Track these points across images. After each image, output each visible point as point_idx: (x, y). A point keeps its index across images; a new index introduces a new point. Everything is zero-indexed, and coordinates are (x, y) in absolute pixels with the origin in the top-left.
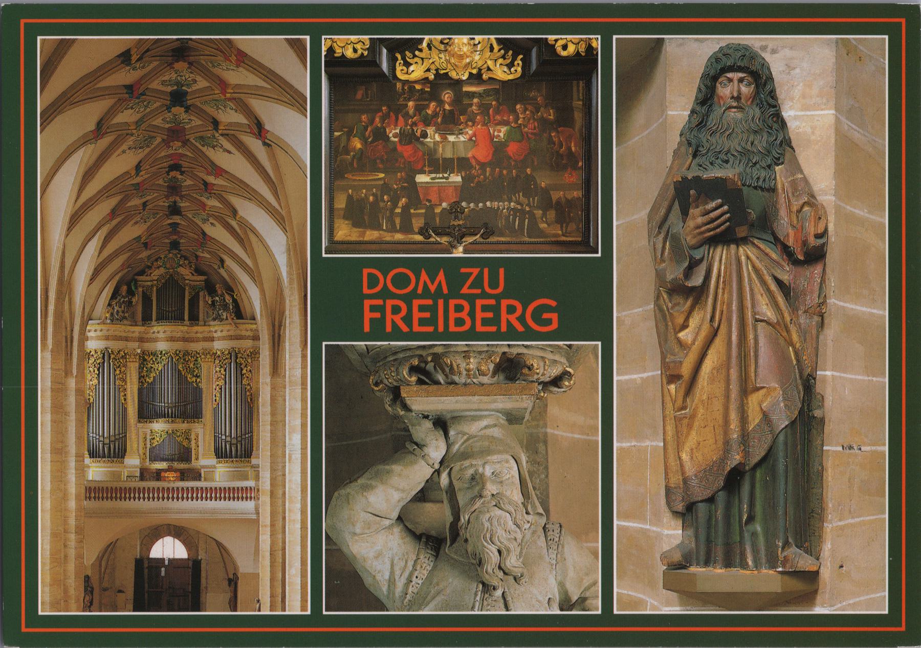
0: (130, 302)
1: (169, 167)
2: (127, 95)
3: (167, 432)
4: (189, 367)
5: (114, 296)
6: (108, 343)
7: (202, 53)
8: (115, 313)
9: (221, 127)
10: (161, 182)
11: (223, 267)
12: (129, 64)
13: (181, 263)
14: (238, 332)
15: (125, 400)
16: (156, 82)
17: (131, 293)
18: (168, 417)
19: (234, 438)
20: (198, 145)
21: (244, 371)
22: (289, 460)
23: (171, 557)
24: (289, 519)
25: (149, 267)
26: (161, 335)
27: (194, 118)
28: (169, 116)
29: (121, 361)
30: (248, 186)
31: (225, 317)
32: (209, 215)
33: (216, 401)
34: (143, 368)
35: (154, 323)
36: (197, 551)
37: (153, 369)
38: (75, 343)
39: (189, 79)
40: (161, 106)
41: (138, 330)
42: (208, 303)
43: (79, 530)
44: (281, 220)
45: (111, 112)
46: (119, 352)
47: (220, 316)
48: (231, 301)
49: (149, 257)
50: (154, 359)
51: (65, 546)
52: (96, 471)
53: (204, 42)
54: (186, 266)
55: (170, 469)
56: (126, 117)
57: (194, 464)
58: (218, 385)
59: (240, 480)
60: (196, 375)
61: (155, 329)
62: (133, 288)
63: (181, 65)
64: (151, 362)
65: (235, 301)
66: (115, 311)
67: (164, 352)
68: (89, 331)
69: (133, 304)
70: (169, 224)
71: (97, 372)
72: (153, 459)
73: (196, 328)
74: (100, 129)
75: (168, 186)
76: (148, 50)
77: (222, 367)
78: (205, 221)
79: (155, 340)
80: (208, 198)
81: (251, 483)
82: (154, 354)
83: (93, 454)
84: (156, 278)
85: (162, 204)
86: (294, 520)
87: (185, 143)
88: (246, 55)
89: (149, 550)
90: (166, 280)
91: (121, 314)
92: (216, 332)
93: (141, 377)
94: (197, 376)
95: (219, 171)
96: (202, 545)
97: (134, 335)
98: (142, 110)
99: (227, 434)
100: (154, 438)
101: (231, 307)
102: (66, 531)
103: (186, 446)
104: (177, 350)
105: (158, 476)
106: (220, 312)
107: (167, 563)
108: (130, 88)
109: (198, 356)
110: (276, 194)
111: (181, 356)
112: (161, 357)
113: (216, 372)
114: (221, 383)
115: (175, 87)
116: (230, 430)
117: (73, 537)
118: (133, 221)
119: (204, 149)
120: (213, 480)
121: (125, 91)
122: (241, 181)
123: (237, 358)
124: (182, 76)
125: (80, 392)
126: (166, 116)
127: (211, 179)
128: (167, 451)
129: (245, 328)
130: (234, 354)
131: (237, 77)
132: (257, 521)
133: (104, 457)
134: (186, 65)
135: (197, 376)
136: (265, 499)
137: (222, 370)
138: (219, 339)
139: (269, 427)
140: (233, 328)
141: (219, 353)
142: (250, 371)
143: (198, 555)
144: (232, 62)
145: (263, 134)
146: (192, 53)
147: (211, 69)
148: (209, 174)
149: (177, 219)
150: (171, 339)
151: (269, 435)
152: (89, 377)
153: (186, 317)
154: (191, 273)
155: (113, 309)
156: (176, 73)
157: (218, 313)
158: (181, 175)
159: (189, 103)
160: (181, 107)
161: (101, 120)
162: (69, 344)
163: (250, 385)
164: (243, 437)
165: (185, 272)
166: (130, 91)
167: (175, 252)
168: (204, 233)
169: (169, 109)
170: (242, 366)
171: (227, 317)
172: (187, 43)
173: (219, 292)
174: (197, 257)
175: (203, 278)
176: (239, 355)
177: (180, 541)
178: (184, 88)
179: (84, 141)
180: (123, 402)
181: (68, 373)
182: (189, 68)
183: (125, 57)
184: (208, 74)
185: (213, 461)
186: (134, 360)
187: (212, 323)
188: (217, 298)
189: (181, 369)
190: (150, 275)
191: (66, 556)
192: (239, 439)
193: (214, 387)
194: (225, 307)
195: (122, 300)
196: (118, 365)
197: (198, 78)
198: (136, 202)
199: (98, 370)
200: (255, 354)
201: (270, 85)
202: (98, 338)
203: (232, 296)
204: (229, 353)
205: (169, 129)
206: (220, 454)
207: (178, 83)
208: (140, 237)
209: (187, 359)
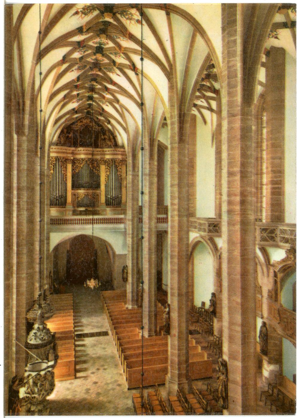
10: (86, 85)
21: (118, 169)
28: (94, 57)
32: (106, 101)
40: (91, 53)
71: (53, 167)
79: (80, 154)
80: (106, 94)
81: (122, 216)
87: (100, 70)
92: (106, 151)
93: (73, 170)
97: (69, 151)
100: (79, 197)
115: (98, 45)
119: (108, 73)
123: (115, 163)
127: (110, 86)
128: (86, 201)
133: (56, 205)
137: (109, 168)
141: (107, 160)
145: (136, 70)
168: (103, 109)
169: (95, 54)
176: (116, 162)
198: (75, 93)
199: (54, 166)
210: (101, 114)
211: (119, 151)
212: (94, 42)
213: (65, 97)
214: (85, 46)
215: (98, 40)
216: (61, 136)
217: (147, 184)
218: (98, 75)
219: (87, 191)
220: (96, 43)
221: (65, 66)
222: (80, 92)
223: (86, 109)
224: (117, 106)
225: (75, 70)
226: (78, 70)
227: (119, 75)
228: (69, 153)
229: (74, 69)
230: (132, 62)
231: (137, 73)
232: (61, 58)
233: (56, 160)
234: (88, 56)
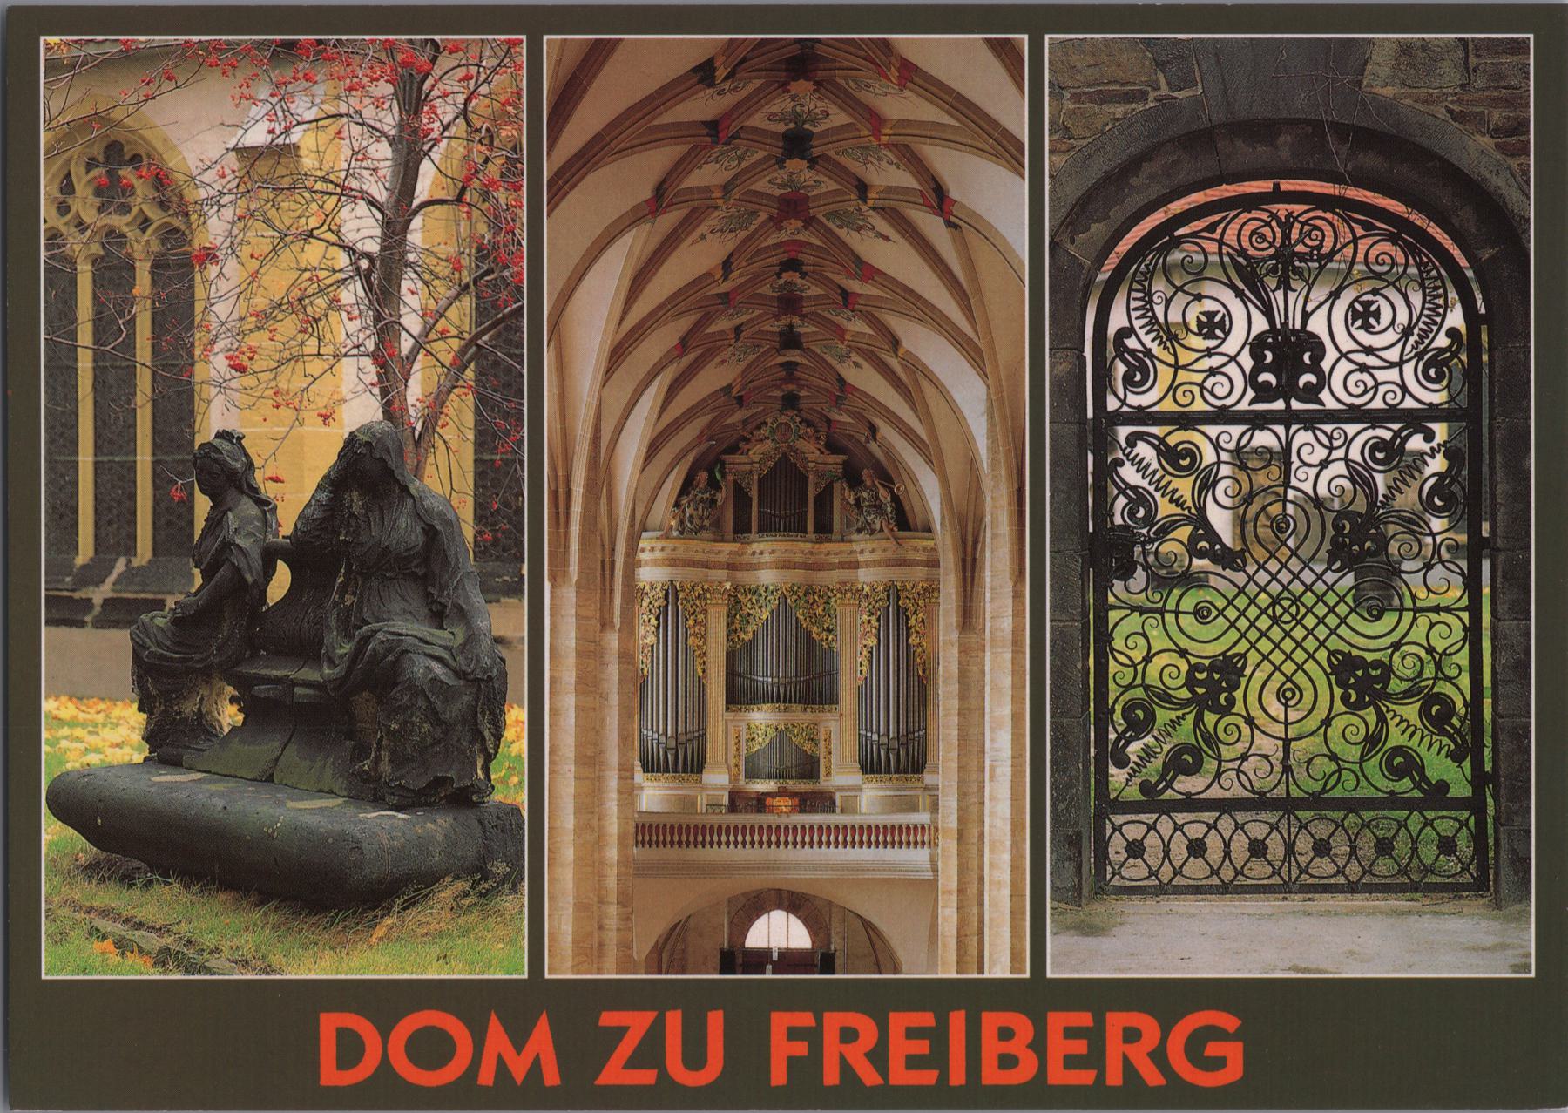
0: (713, 501)
1: (781, 264)
2: (708, 139)
5: (684, 491)
7: (838, 65)
9: (872, 195)
10: (766, 290)
11: (875, 440)
12: (711, 85)
13: (801, 432)
14: (901, 553)
15: (704, 671)
16: (758, 116)
17: (714, 485)
18: (778, 701)
20: (830, 225)
21: (912, 622)
23: (783, 945)
24: (991, 881)
25: (748, 440)
26: (767, 558)
27: (825, 179)
28: (781, 176)
29: (697, 602)
30: (919, 297)
31: (878, 527)
35: (753, 536)
36: (829, 936)
38: (619, 573)
39: (817, 111)
40: (767, 159)
41: (727, 548)
42: (848, 503)
43: (624, 900)
44: (975, 355)
45: (680, 167)
46: (693, 588)
48: (889, 499)
49: (745, 422)
51: (601, 927)
52: (653, 795)
53: (837, 44)
55: (782, 793)
56: (707, 175)
57: (824, 783)
59: (900, 810)
61: (756, 547)
62: (718, 477)
63: (802, 87)
65: (896, 499)
68: (643, 550)
69: (719, 503)
70: (781, 365)
71: (654, 622)
72: (752, 775)
73: (827, 546)
74: (659, 200)
75: (779, 298)
76: (744, 60)
78: (843, 358)
80: (849, 320)
81: (923, 818)
82: (754, 592)
83: (649, 767)
84: (756, 459)
85: (767, 328)
86: (999, 882)
87: (809, 222)
88: (916, 69)
89: (744, 935)
91: (696, 521)
92: (862, 552)
93: (731, 631)
94: (829, 630)
95: (867, 272)
96: (836, 927)
98: (734, 164)
101: (889, 509)
102: (601, 901)
103: (809, 752)
105: (760, 803)
106: (869, 518)
107: (775, 956)
108: (713, 127)
110: (967, 310)
114: (872, 642)
115: (792, 125)
116: (884, 725)
117: (613, 910)
118: (718, 359)
119: (842, 233)
120: (854, 811)
121: (705, 132)
122: (911, 291)
124: (803, 106)
125: (626, 657)
126: (775, 175)
127: (855, 286)
129: (916, 546)
130: (894, 591)
131: (900, 106)
132: (932, 885)
134: (810, 85)
135: (829, 630)
136: (948, 846)
137: (873, 619)
138: (867, 564)
140: (891, 544)
143: (829, 943)
144: (889, 79)
146: (821, 66)
147: (855, 94)
148: (853, 277)
149: (794, 356)
150: (786, 565)
152: (642, 631)
153: (810, 526)
155: (684, 511)
156: (793, 100)
158: (802, 278)
159: (816, 152)
160: (802, 158)
161: (664, 181)
162: (607, 572)
164: (910, 736)
165: (811, 451)
166: (714, 132)
167: (791, 413)
168: (841, 380)
169: (781, 163)
170: (908, 613)
172: (813, 47)
173: (868, 483)
174: (829, 421)
175: (841, 458)
176: (903, 594)
177: (799, 918)
178: (806, 126)
179: (633, 219)
181: (606, 624)
182: (815, 91)
183: (704, 73)
184: (850, 102)
185: (854, 778)
187: (855, 537)
188: (865, 494)
189: (802, 618)
191: (601, 945)
192: (903, 740)
194: (878, 507)
197: (833, 109)
198: (722, 324)
199: (658, 618)
200: (931, 590)
201: (957, 119)
202: (655, 563)
203: (891, 490)
204: (885, 590)
205: (781, 199)
206: (869, 766)
207: (797, 118)
208: (730, 387)
210: (838, 402)
211: (915, 549)
212: (775, 114)
213: (683, 345)
214: (736, 136)
215: (782, 104)
216: (684, 501)
218: (802, 244)
219: (788, 716)
220: (782, 117)
221: (668, 220)
222: (745, 318)
223: (778, 387)
224: (894, 363)
225: (710, 236)
226: (722, 231)
227: (887, 238)
229: (703, 229)
230: (934, 179)
231: (952, 219)
232: (647, 194)
234: (754, 170)
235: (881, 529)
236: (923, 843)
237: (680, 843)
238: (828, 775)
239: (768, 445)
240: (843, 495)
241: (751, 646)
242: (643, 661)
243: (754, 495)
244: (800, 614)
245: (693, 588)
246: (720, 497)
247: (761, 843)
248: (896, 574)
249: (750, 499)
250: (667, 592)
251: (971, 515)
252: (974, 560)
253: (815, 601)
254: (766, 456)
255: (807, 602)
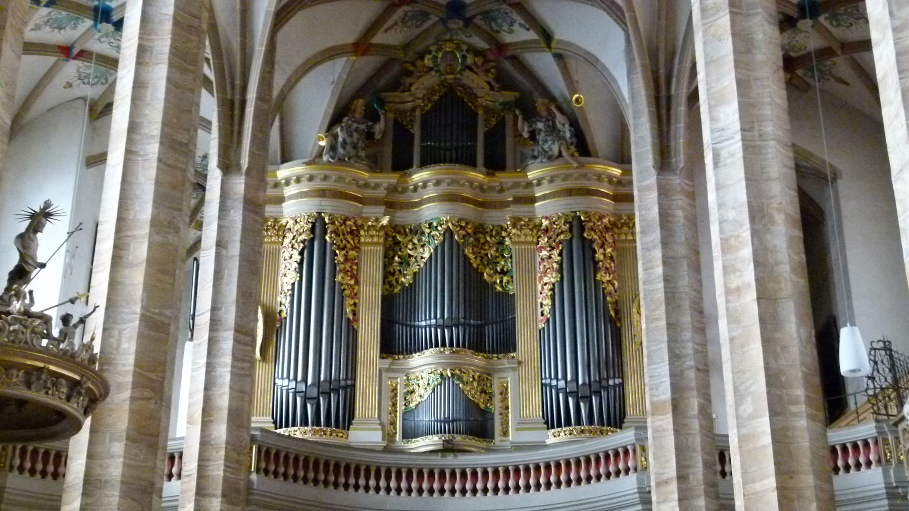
0: (369, 135)
3: (442, 375)
4: (487, 255)
6: (323, 203)
8: (339, 145)
15: (354, 314)
17: (372, 116)
19: (584, 384)
21: (599, 256)
22: (716, 163)
25: (409, 74)
33: (542, 314)
34: (393, 258)
37: (413, 260)
46: (344, 222)
47: (546, 152)
50: (416, 241)
54: (478, 67)
58: (546, 284)
60: (502, 270)
64: (410, 246)
66: (340, 139)
67: (435, 224)
69: (378, 136)
71: (299, 258)
77: (553, 248)
82: (417, 231)
90: (441, 97)
91: (348, 148)
93: (388, 274)
94: (503, 273)
99: (569, 378)
100: (413, 392)
101: (568, 135)
103: (482, 406)
104: (460, 220)
106: (546, 147)
109: (504, 234)
111: (469, 231)
112: (429, 234)
113: (543, 260)
135: (503, 273)
137: (555, 253)
138: (544, 197)
139: (659, 270)
141: (545, 223)
142: (611, 258)
150: (450, 198)
151: (661, 285)
152: (282, 270)
154: (489, 83)
157: (542, 148)
163: (613, 285)
164: (604, 383)
171: (560, 152)
180: (351, 317)
186: (375, 239)
189: (471, 256)
190: (409, 90)
193: (539, 288)
195: (355, 125)
196: (342, 245)
199: (301, 253)
204: (566, 222)
209: (482, 241)
217: (727, 47)
228: (375, 202)
233: (312, 230)
235: (560, 155)
236: (627, 471)
237: (316, 482)
238: (505, 433)
239: (431, 80)
240: (516, 125)
241: (411, 290)
242: (283, 302)
243: (416, 131)
244: (468, 252)
245: (344, 222)
246: (379, 128)
247: (420, 491)
248: (577, 204)
249: (413, 136)
250: (314, 224)
251: (662, 46)
252: (669, 99)
253: (486, 241)
254: (431, 91)
255: (477, 240)
